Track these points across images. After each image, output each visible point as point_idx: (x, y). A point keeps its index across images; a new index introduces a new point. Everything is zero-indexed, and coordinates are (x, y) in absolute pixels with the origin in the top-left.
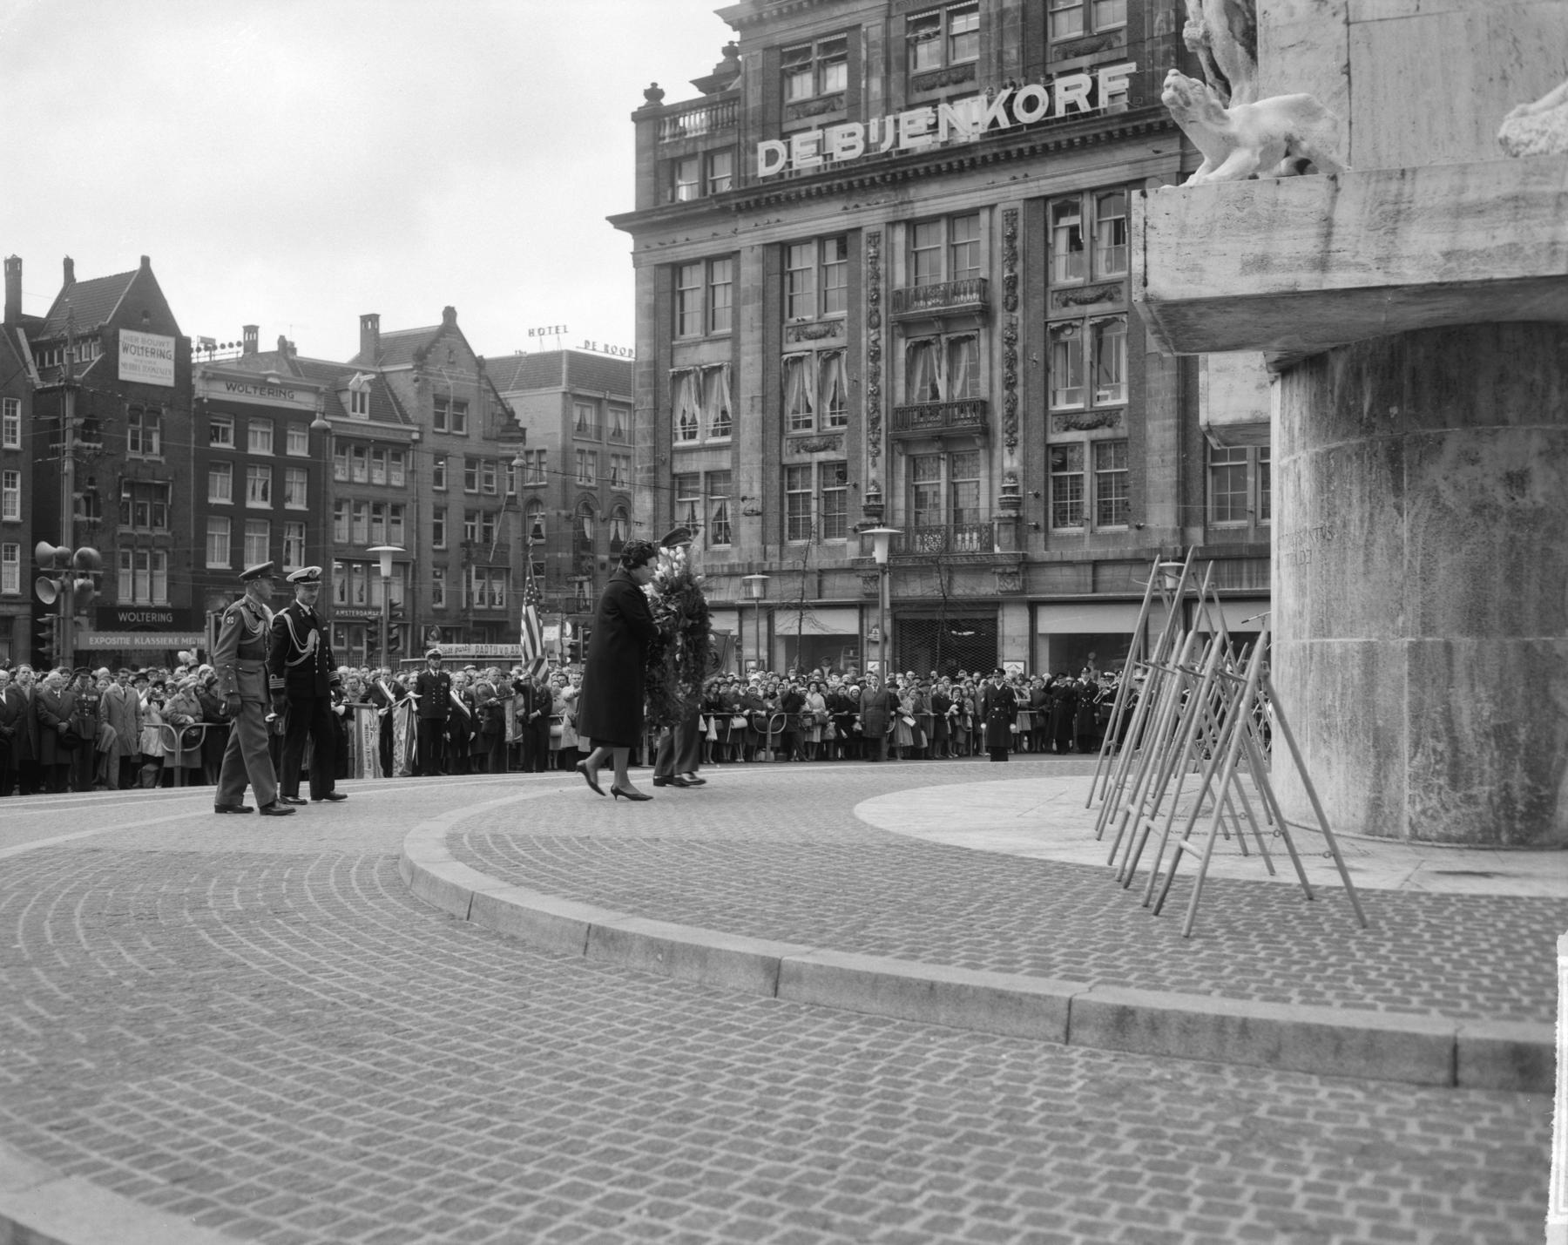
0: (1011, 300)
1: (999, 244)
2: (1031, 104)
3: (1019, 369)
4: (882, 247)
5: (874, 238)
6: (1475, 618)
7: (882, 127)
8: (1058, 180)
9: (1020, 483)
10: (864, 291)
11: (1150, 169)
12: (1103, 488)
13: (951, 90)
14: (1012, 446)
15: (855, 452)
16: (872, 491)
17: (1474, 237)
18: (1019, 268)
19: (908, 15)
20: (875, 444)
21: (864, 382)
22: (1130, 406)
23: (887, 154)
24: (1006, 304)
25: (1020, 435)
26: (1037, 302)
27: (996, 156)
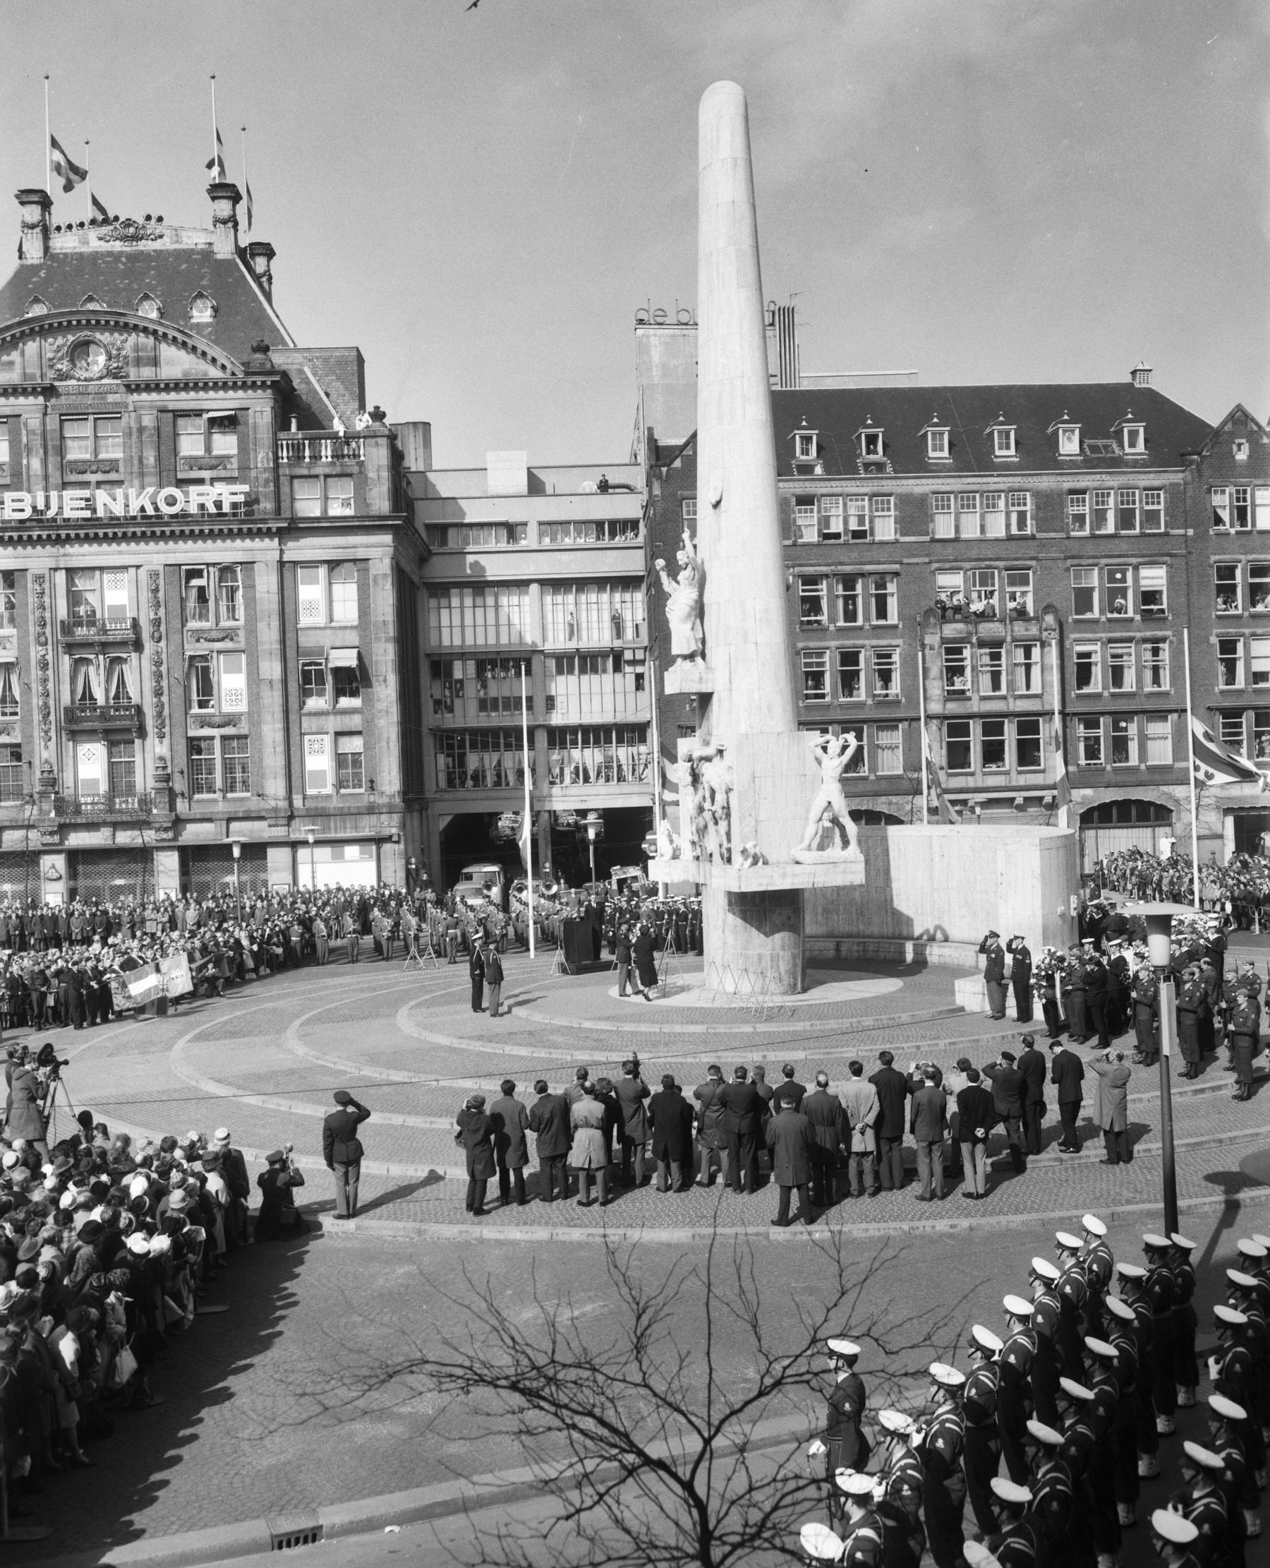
0: (156, 635)
1: (145, 595)
2: (171, 501)
3: (164, 683)
4: (46, 585)
5: (39, 579)
6: (783, 948)
7: (47, 498)
8: (190, 555)
9: (169, 764)
10: (31, 617)
11: (257, 556)
12: (228, 767)
13: (99, 477)
14: (161, 736)
15: (29, 737)
16: (47, 767)
17: (796, 881)
18: (162, 612)
19: (61, 415)
20: (46, 732)
21: (34, 686)
22: (249, 714)
23: (54, 520)
24: (153, 637)
25: (167, 730)
26: (177, 637)
27: (143, 533)
